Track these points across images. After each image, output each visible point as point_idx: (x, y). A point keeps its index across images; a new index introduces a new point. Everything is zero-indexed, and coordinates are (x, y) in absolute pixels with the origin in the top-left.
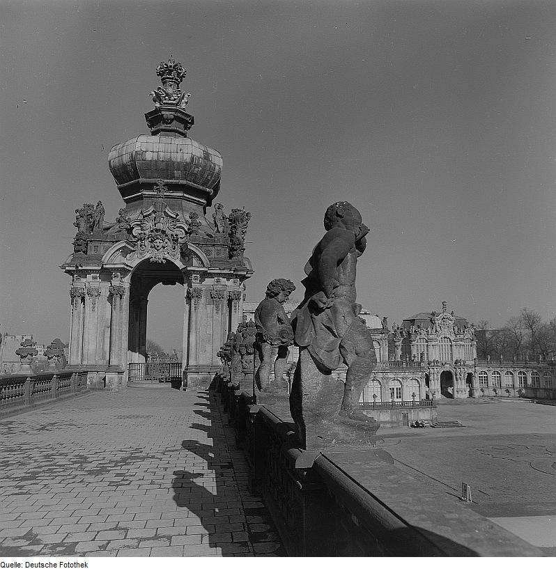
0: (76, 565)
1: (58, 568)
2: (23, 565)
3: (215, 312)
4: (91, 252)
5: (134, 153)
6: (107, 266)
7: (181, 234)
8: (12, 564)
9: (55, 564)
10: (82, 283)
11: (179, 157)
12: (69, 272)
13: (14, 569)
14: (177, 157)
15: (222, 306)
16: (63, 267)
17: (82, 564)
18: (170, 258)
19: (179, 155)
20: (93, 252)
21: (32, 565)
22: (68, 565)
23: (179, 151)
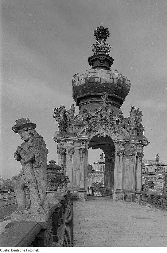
0: (33, 250)
1: (25, 252)
2: (10, 250)
3: (130, 163)
4: (69, 130)
5: (88, 79)
6: (79, 138)
8: (5, 250)
9: (24, 250)
10: (67, 146)
12: (58, 141)
13: (6, 252)
14: (110, 81)
17: (36, 250)
18: (108, 135)
21: (14, 250)
22: (30, 250)
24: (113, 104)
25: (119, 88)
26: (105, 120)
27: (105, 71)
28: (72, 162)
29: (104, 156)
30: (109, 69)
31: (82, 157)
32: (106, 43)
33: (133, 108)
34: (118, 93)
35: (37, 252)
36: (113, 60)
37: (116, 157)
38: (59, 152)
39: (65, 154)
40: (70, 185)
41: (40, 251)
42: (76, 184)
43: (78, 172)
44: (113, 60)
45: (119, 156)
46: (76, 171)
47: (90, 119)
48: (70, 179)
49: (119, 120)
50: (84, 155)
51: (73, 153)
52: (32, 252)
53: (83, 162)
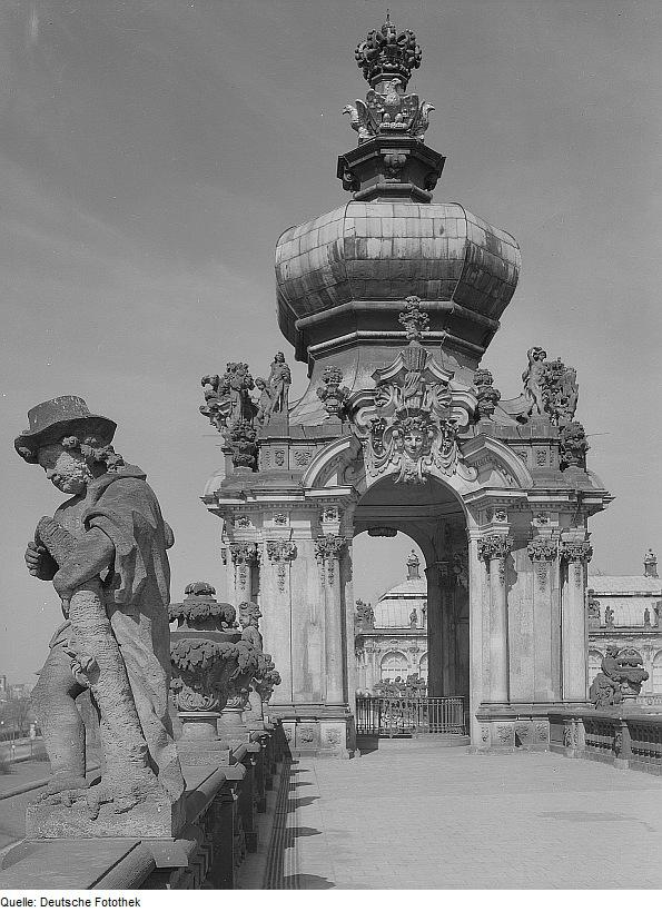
0: (121, 902)
1: (92, 908)
2: (37, 903)
7: (462, 419)
8: (19, 901)
9: (88, 902)
11: (439, 248)
12: (223, 512)
13: (23, 909)
14: (436, 248)
15: (553, 575)
16: (207, 500)
17: (131, 901)
18: (436, 472)
19: (439, 242)
20: (273, 466)
21: (51, 903)
22: (108, 903)
23: (437, 234)
24: (448, 345)
25: (474, 275)
26: (413, 412)
27: (407, 207)
28: (286, 596)
29: (423, 565)
30: (426, 200)
31: (327, 574)
32: (410, 92)
33: (538, 355)
34: (471, 300)
35: (135, 909)
36: (441, 160)
37: (476, 566)
38: (230, 556)
39: (254, 564)
40: (280, 694)
41: (144, 906)
42: (307, 687)
43: (315, 639)
44: (441, 160)
45: (487, 560)
46: (305, 630)
47: (357, 409)
48: (281, 666)
49: (477, 408)
50: (336, 563)
51: (293, 556)
52: (118, 909)
53: (333, 593)
